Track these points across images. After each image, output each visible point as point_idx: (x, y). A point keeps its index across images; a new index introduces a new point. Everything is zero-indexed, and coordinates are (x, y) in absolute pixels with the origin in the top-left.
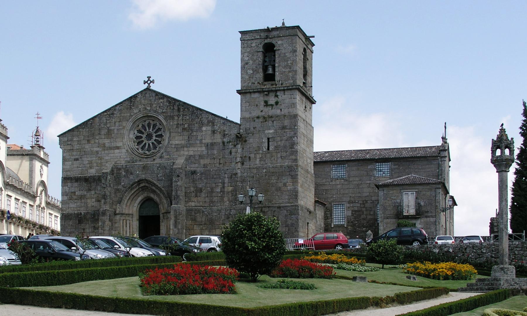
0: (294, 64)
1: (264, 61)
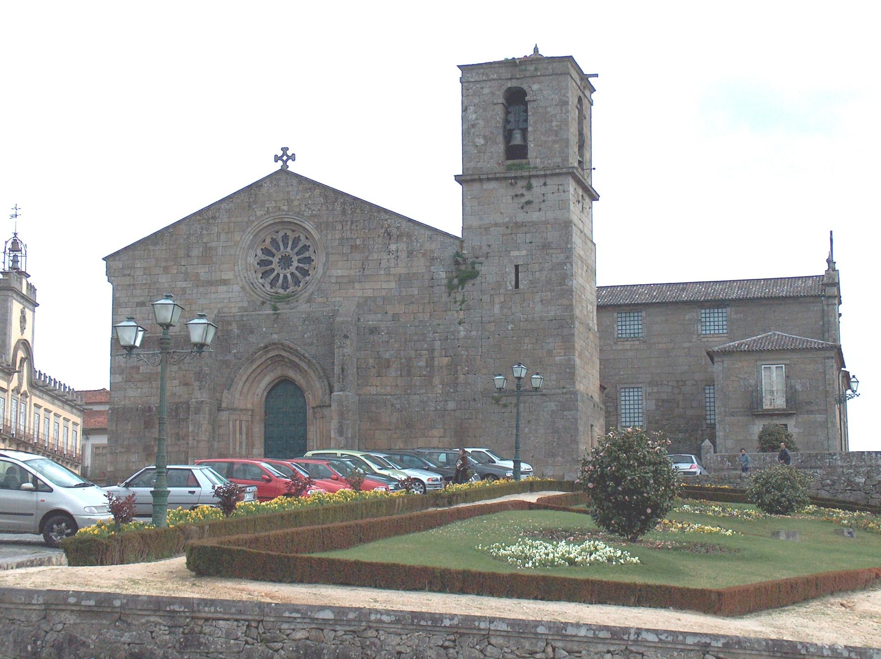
0: (563, 127)
1: (507, 121)
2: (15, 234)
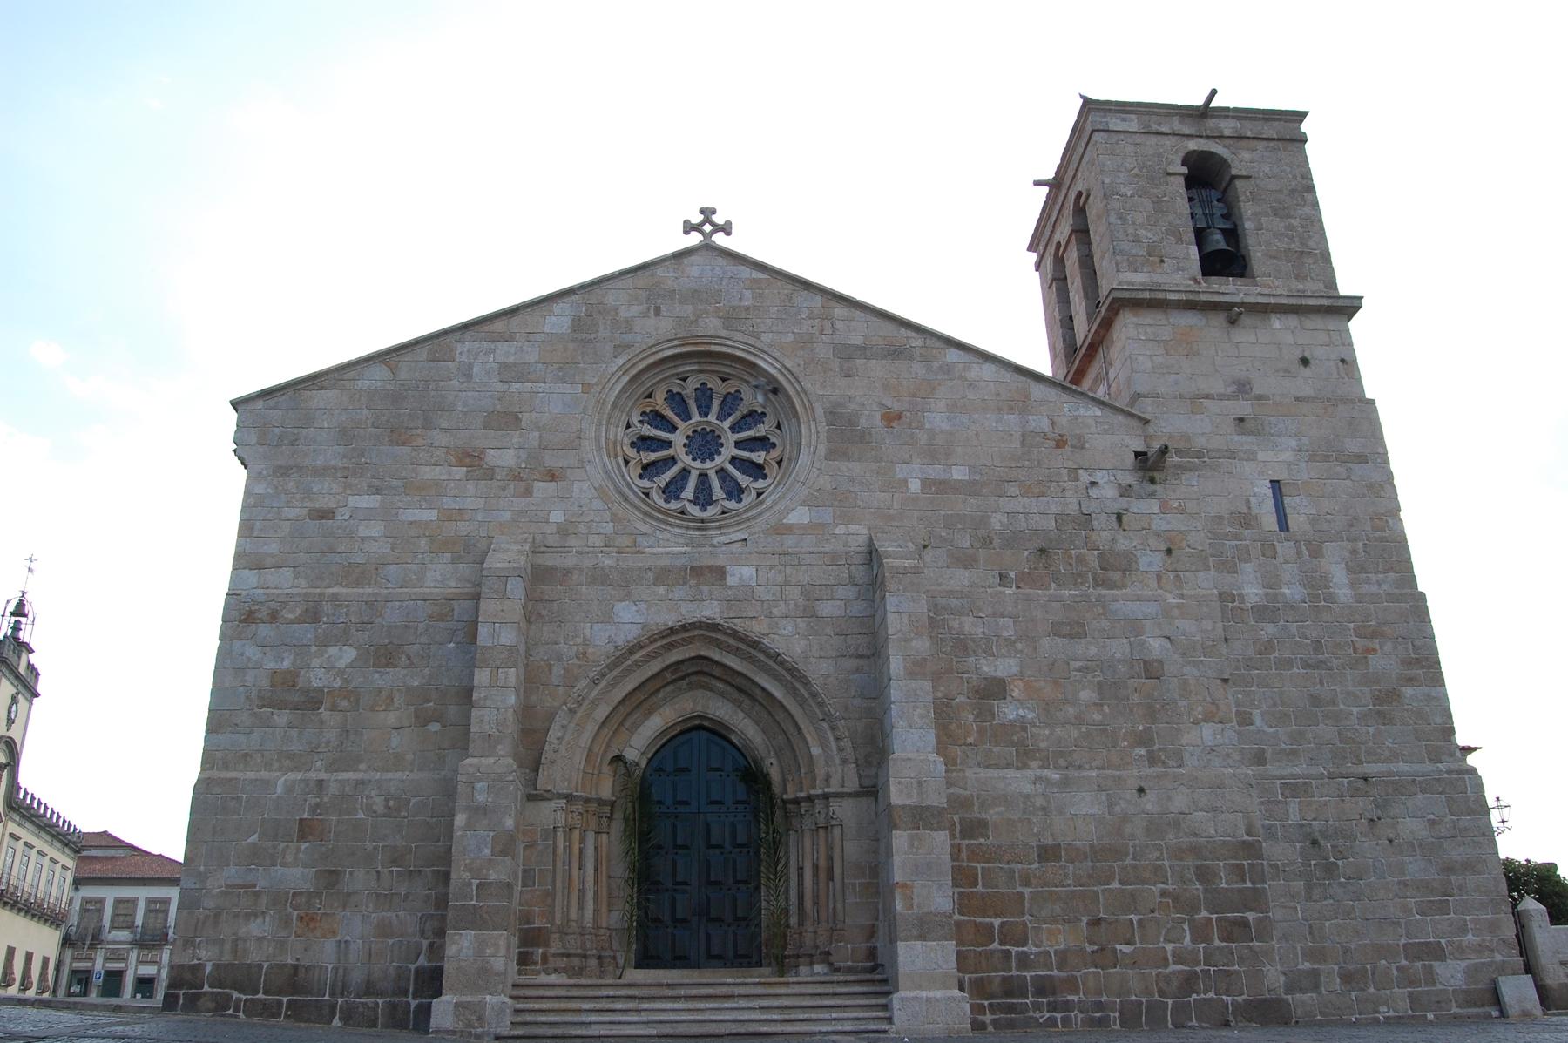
2: (24, 593)
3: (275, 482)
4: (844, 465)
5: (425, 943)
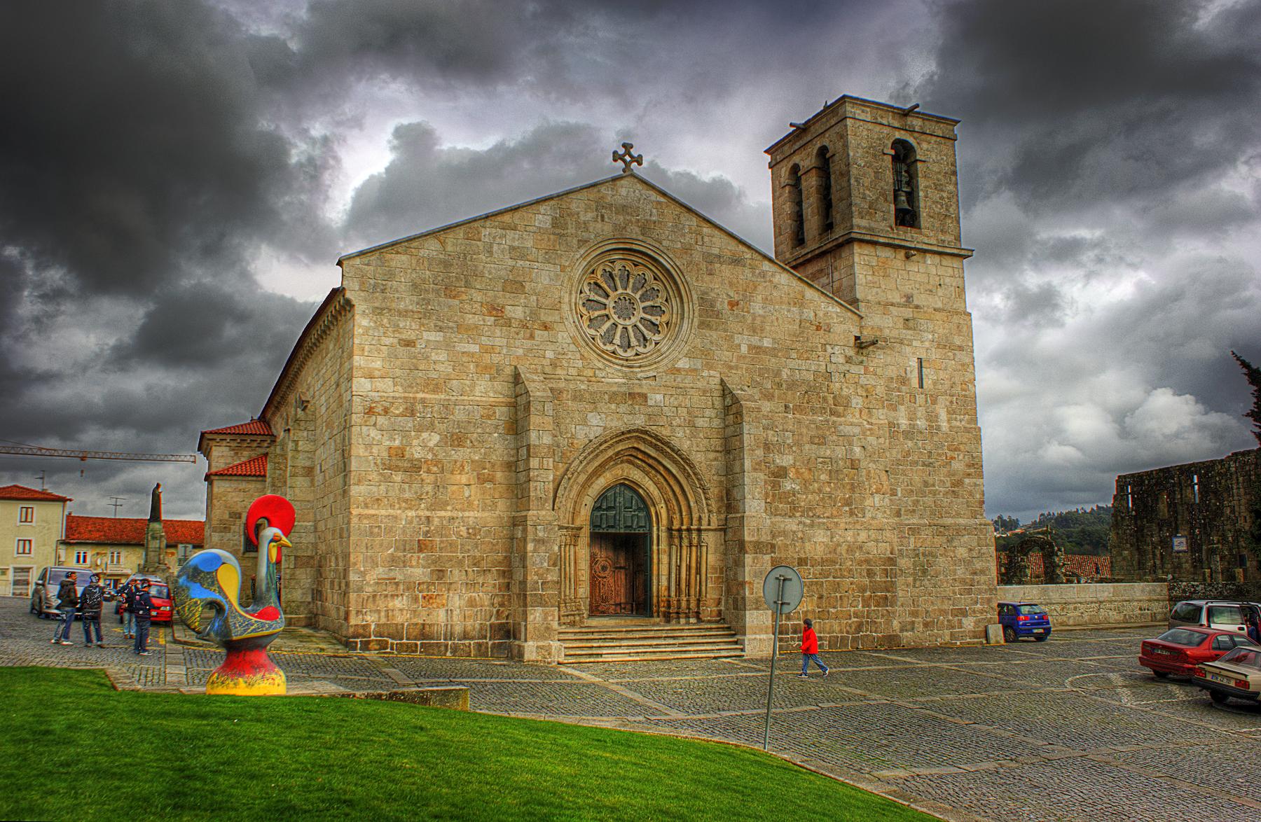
3: (374, 319)
4: (707, 332)
5: (495, 610)
